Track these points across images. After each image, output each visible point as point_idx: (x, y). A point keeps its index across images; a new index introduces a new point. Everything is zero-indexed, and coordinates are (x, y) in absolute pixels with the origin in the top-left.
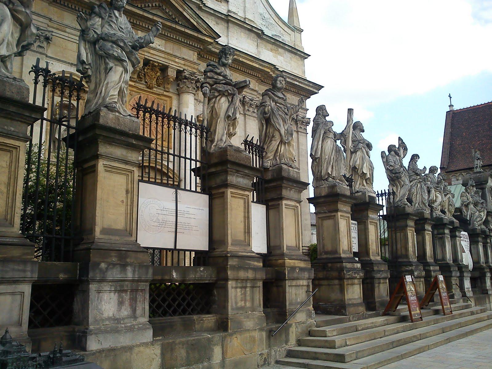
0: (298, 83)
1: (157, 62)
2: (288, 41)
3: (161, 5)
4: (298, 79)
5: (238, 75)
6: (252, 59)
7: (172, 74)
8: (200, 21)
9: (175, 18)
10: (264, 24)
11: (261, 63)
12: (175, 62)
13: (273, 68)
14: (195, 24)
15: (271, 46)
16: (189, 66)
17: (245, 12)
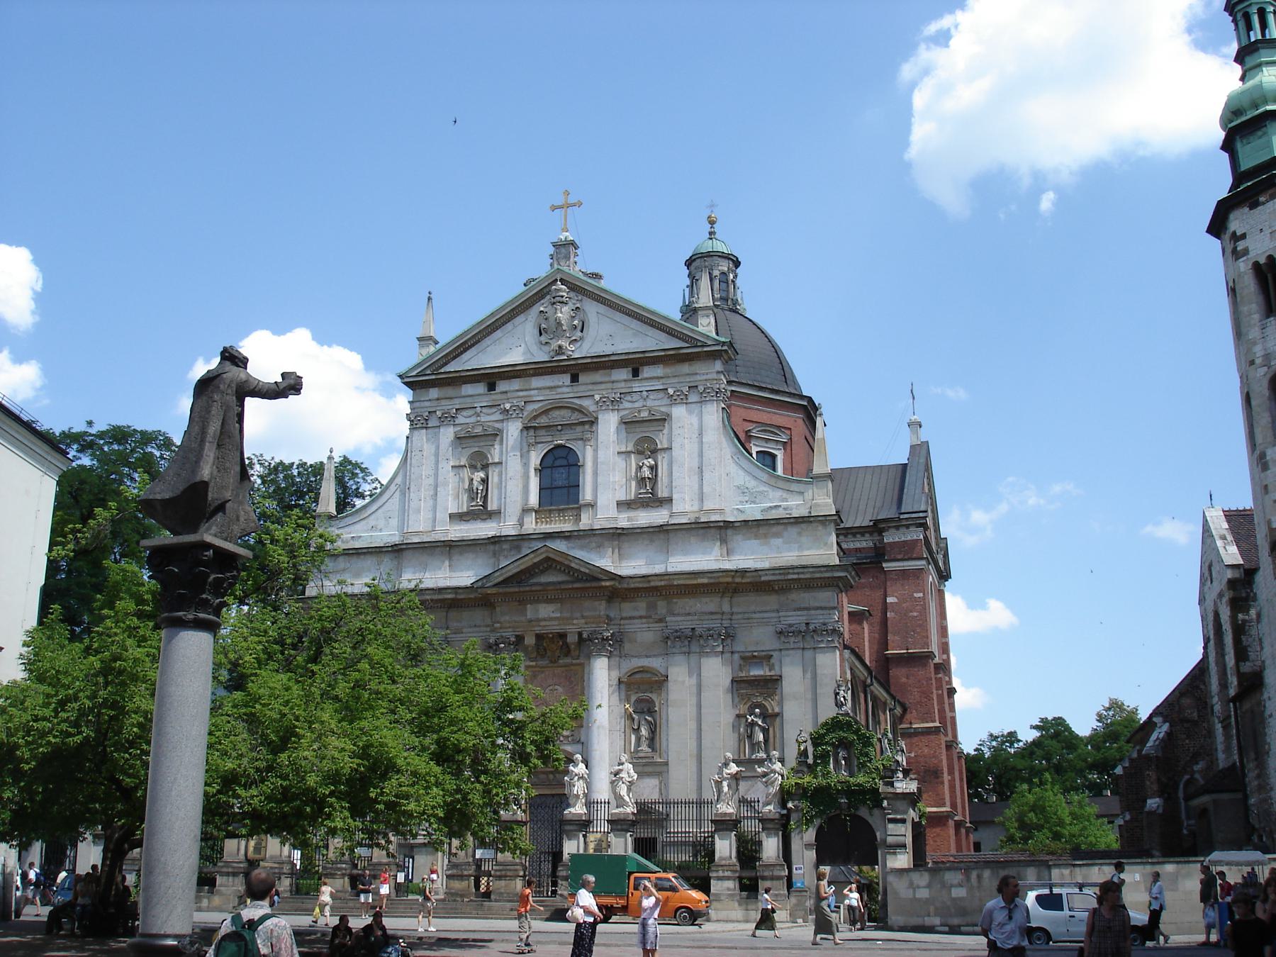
0: (795, 576)
1: (551, 633)
2: (798, 505)
3: (550, 564)
4: (791, 571)
5: (687, 600)
6: (693, 576)
7: (572, 639)
8: (592, 567)
9: (569, 572)
10: (747, 498)
11: (709, 575)
12: (573, 624)
13: (733, 574)
14: (587, 571)
15: (755, 530)
16: (593, 623)
17: (702, 500)
